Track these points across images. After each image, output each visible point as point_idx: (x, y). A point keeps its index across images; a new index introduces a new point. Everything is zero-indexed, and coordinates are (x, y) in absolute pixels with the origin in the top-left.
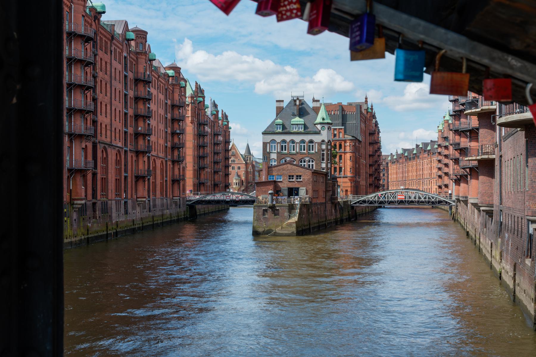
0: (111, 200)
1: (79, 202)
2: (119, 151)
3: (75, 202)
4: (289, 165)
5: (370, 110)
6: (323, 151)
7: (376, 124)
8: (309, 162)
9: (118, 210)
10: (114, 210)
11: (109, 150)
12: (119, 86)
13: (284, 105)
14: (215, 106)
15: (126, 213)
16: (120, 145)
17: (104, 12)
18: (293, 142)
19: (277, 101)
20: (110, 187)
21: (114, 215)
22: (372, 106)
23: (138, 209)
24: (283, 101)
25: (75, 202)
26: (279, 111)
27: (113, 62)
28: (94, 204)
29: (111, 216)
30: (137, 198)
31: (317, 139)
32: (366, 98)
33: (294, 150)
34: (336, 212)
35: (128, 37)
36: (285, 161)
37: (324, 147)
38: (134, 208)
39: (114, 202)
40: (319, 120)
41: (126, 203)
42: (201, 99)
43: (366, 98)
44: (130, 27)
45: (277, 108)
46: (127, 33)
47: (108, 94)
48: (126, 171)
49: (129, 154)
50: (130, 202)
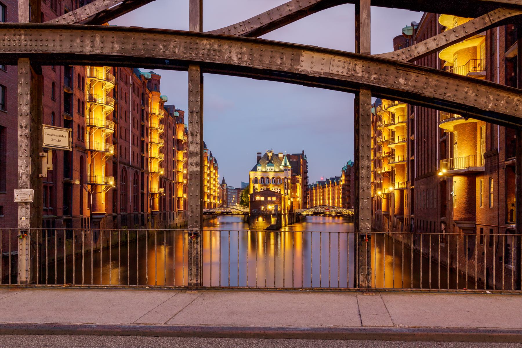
0: (167, 212)
1: (155, 213)
2: (170, 183)
3: (154, 213)
4: (268, 192)
5: (305, 159)
6: (286, 183)
7: (307, 166)
8: (278, 189)
9: (170, 218)
10: (168, 218)
11: (166, 182)
12: (170, 144)
13: (262, 155)
14: (211, 155)
15: (174, 220)
16: (171, 179)
17: (167, 101)
18: (268, 178)
19: (258, 153)
20: (167, 204)
21: (169, 220)
22: (305, 156)
23: (178, 217)
24: (261, 153)
25: (154, 213)
26: (259, 159)
27: (169, 130)
28: (160, 214)
29: (167, 221)
30: (178, 210)
31: (282, 176)
32: (303, 151)
33: (268, 182)
34: (291, 219)
35: (175, 115)
36: (263, 189)
37: (286, 181)
38: (177, 217)
39: (168, 213)
40: (283, 164)
41: (173, 213)
42: (206, 151)
43: (303, 151)
44: (176, 108)
45: (258, 157)
46: (175, 113)
47: (166, 149)
48: (174, 196)
49: (175, 185)
50: (175, 213)
